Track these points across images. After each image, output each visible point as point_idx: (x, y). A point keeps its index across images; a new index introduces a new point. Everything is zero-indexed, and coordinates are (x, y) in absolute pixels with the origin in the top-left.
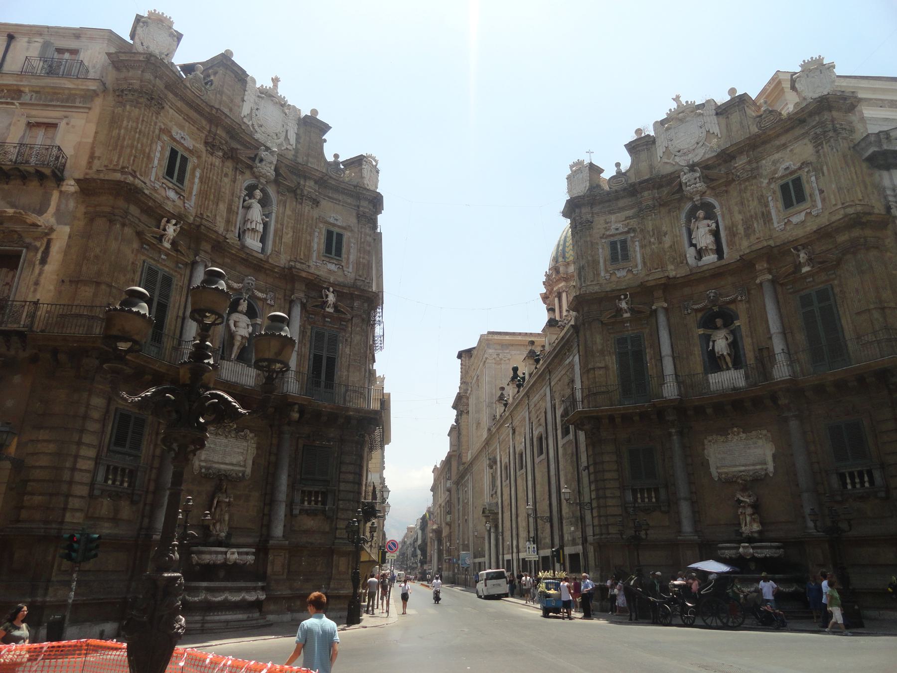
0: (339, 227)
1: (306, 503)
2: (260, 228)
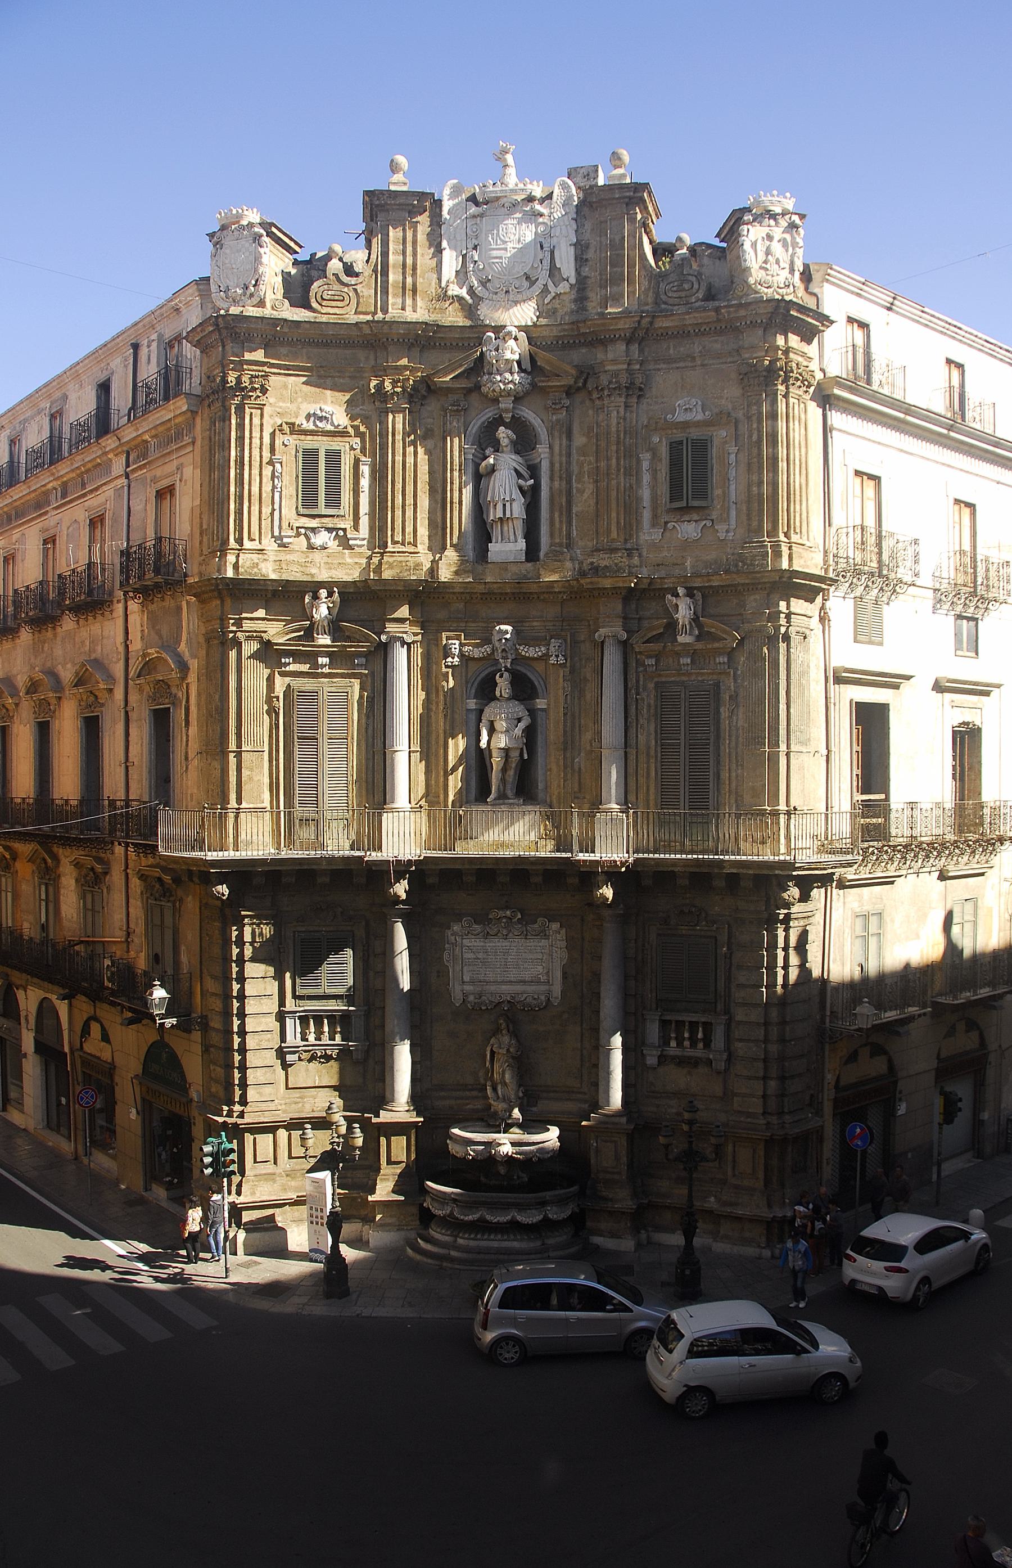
0: (698, 424)
1: (673, 1044)
2: (518, 509)
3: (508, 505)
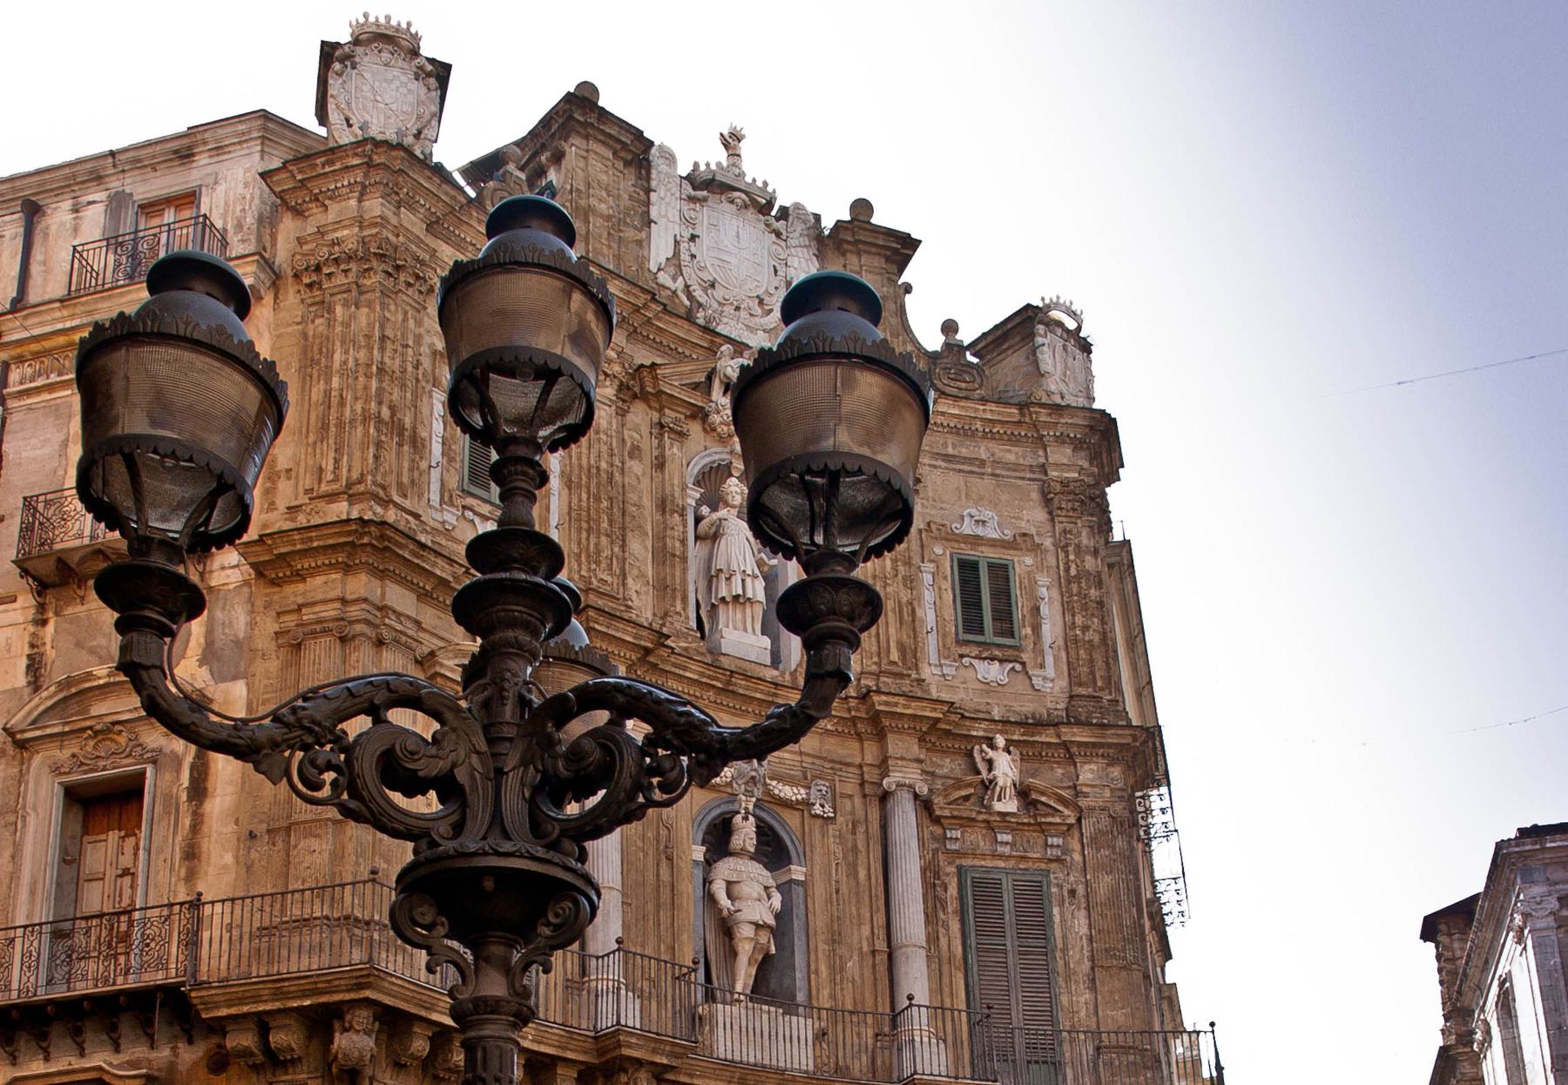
0: (993, 543)
3: (748, 580)
